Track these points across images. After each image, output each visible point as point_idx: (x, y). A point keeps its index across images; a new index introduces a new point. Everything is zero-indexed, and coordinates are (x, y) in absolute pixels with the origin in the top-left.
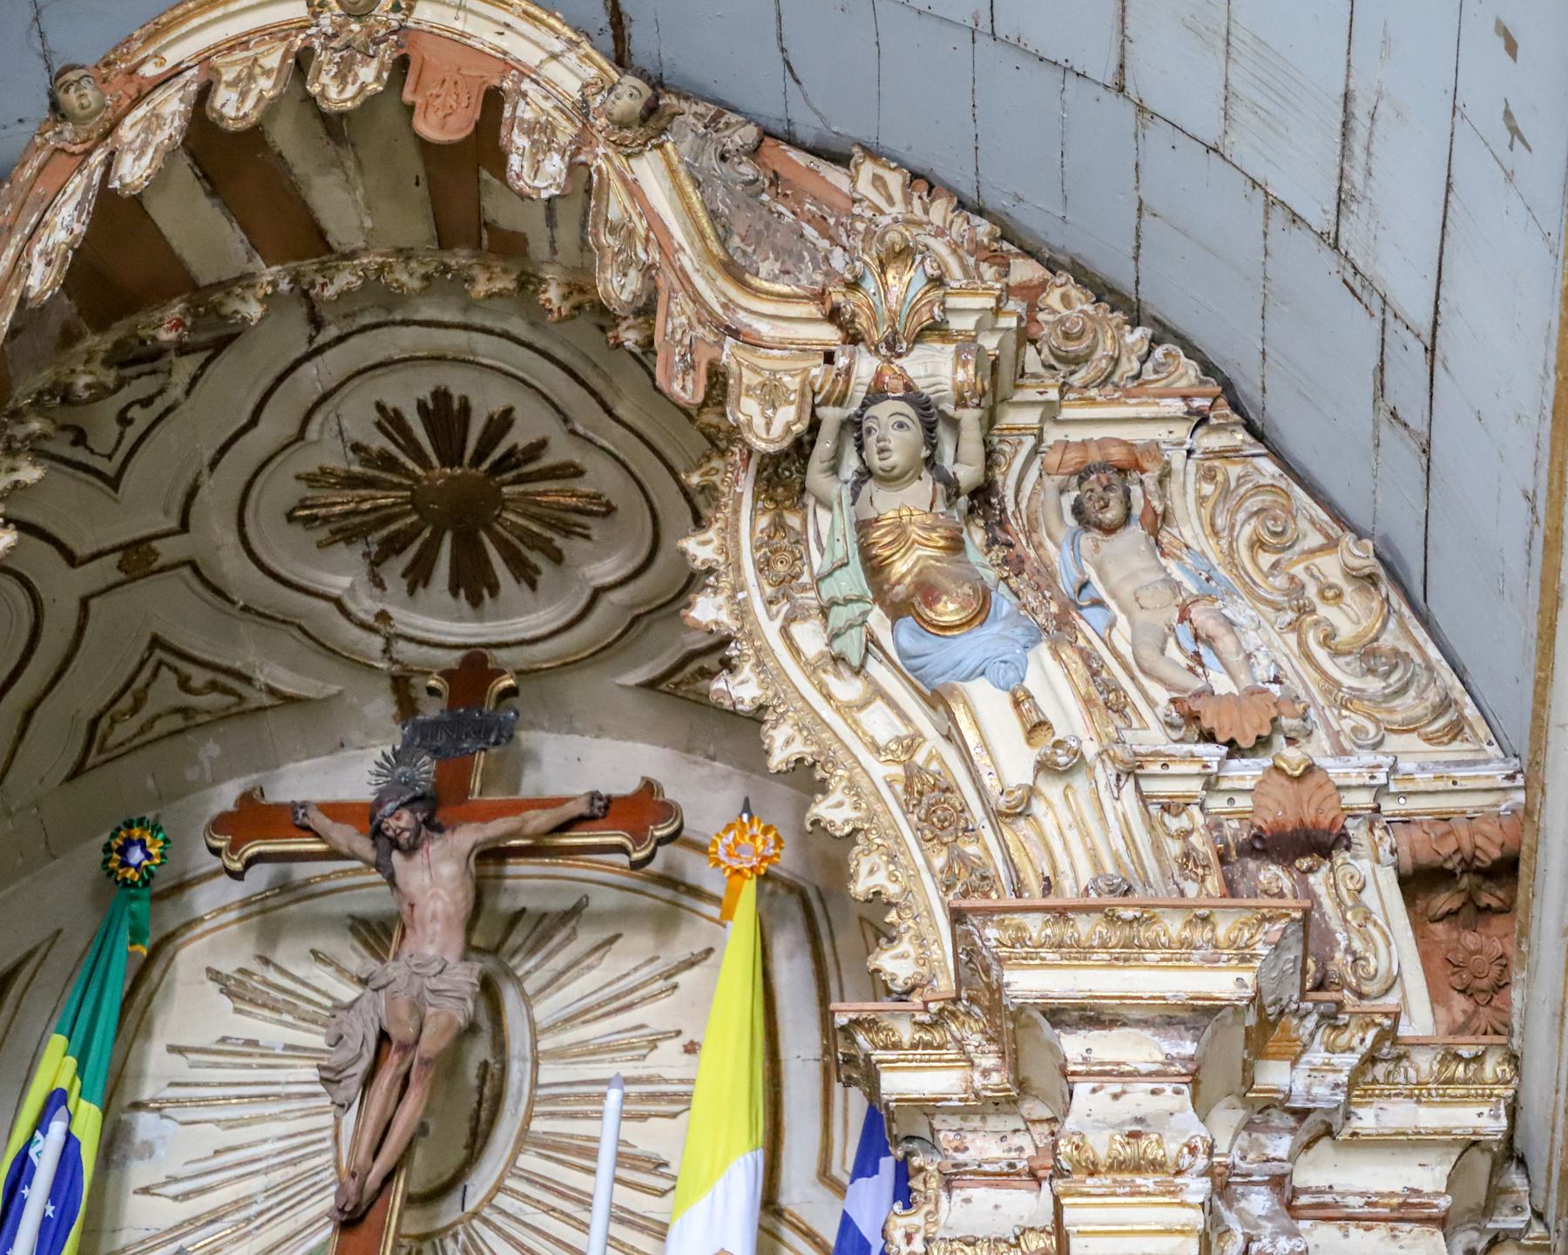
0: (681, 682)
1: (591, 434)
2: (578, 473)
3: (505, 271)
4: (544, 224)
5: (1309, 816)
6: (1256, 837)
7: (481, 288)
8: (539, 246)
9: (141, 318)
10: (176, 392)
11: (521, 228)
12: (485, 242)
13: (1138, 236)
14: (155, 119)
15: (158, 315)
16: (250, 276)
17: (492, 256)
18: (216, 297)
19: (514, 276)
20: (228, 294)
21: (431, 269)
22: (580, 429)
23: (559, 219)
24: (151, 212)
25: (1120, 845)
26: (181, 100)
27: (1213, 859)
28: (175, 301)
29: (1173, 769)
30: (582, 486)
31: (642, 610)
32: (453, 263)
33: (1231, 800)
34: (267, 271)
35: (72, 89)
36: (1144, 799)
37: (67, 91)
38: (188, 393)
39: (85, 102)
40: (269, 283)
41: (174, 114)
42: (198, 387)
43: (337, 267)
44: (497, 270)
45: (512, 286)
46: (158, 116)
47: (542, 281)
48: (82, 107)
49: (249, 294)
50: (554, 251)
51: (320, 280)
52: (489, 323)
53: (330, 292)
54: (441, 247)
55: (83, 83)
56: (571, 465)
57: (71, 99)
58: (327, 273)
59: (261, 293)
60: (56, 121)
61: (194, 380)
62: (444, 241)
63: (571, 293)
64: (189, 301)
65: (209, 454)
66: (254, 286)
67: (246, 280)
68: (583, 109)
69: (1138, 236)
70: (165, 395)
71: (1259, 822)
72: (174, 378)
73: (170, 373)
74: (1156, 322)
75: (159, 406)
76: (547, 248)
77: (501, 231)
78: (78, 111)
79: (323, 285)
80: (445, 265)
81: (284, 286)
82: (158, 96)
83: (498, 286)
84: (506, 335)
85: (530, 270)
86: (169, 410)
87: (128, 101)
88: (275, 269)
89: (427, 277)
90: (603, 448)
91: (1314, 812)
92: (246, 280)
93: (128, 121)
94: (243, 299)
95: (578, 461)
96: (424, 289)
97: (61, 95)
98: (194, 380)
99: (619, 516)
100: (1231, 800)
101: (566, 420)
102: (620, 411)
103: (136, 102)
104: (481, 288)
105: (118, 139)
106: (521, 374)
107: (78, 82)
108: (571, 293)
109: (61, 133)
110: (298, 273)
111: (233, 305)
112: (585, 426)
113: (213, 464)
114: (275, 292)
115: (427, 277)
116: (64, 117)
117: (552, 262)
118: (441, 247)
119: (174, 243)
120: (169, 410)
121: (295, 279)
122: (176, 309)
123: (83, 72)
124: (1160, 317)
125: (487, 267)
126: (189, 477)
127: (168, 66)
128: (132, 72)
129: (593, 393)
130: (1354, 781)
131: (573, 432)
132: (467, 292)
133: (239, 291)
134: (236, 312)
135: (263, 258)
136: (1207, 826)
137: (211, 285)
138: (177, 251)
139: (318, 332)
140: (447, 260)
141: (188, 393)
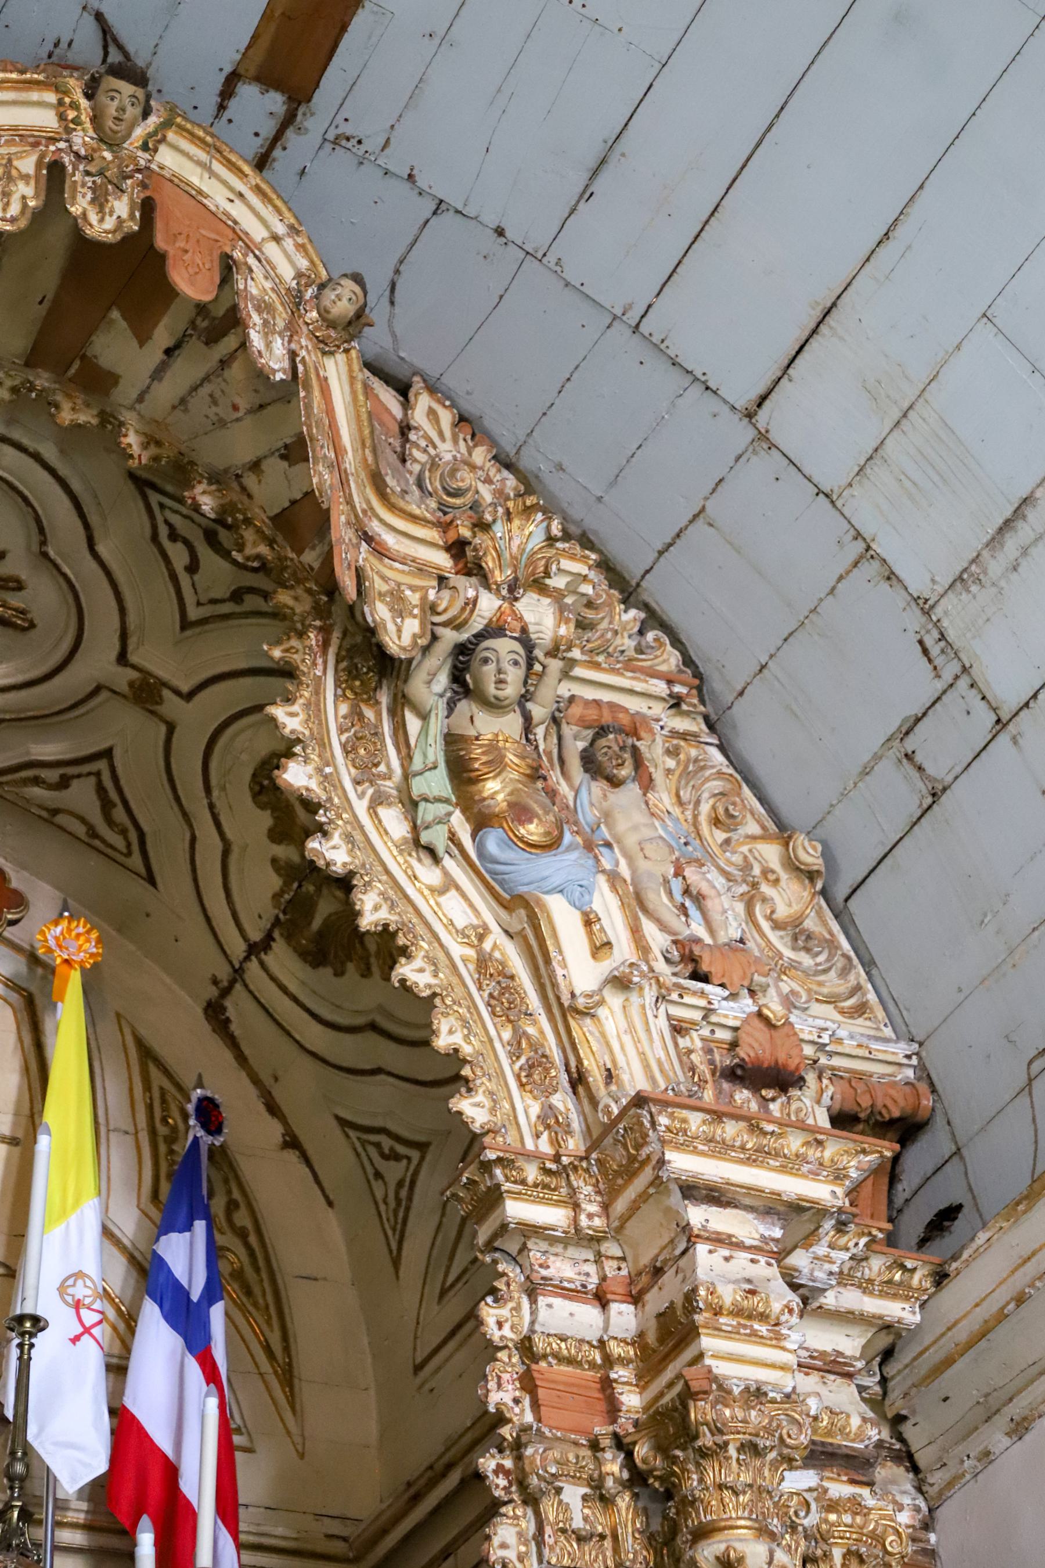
0: (7, 783)
1: (59, 561)
2: (19, 586)
3: (88, 405)
4: (149, 374)
5: (782, 1057)
6: (738, 1065)
7: (66, 416)
8: (125, 392)
11: (119, 371)
12: (72, 371)
13: (678, 536)
17: (72, 385)
19: (95, 412)
21: (17, 382)
22: (52, 553)
23: (169, 374)
25: (662, 1055)
27: (708, 1077)
29: (687, 999)
30: (15, 600)
31: (7, 717)
32: (37, 382)
33: (713, 1032)
36: (669, 1017)
44: (79, 401)
45: (95, 421)
47: (122, 424)
50: (141, 399)
52: (25, 441)
54: (27, 364)
56: (18, 581)
62: (32, 360)
63: (148, 443)
68: (296, 301)
69: (678, 536)
71: (742, 1055)
74: (646, 607)
76: (134, 395)
77: (97, 368)
80: (29, 382)
83: (82, 418)
84: (36, 457)
85: (108, 410)
89: (14, 390)
90: (64, 575)
91: (784, 1055)
95: (23, 577)
96: (11, 402)
99: (32, 634)
100: (713, 1032)
101: (44, 543)
102: (101, 549)
104: (66, 416)
106: (26, 493)
108: (148, 443)
112: (58, 553)
115: (14, 390)
117: (132, 408)
118: (27, 364)
124: (654, 605)
125: (69, 396)
129: (87, 526)
130: (807, 1037)
131: (45, 555)
132: (52, 416)
136: (703, 1049)
140: (31, 379)
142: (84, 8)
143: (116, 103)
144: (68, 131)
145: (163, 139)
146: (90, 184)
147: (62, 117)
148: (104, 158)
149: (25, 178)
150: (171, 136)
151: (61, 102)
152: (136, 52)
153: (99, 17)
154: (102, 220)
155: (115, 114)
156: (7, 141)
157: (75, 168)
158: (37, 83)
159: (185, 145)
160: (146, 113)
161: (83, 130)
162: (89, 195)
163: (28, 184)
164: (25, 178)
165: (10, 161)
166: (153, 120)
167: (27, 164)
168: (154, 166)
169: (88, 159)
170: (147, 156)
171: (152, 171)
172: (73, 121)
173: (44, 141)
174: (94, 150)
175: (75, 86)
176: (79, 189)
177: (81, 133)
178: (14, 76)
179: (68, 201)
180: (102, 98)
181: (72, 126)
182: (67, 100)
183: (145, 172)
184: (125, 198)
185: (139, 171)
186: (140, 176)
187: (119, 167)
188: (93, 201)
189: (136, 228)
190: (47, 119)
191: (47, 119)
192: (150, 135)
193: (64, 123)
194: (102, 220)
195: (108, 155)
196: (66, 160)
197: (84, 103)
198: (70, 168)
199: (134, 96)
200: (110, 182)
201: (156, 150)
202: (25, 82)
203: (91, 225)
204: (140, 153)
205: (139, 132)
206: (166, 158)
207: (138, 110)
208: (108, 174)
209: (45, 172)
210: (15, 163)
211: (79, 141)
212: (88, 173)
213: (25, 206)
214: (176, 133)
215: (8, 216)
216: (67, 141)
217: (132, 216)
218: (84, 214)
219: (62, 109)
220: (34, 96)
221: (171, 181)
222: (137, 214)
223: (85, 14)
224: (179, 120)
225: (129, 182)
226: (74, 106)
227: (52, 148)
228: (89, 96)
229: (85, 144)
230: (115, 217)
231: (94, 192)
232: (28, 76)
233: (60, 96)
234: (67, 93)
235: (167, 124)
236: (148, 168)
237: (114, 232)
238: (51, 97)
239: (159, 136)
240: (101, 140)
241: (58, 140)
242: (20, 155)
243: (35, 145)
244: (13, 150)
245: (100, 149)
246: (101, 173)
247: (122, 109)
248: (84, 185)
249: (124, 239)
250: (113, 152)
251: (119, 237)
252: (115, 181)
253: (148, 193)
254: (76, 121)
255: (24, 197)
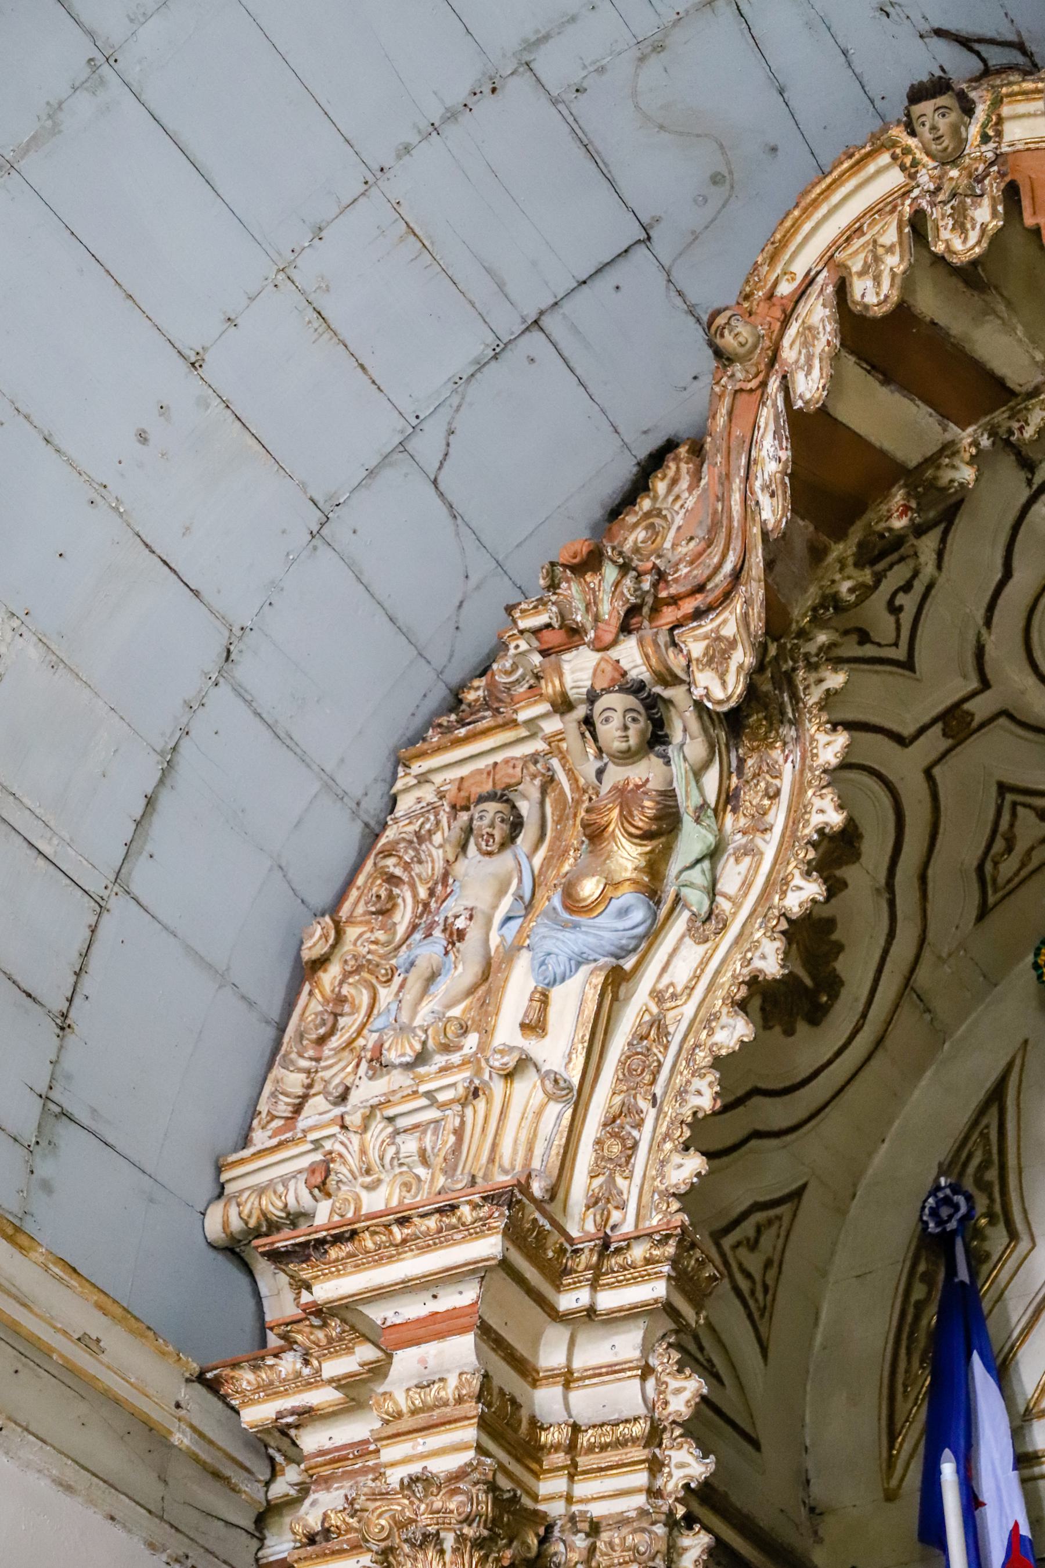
9: (870, 516)
10: (929, 569)
14: (809, 332)
15: (884, 508)
16: (952, 443)
18: (929, 473)
20: (938, 467)
24: (840, 418)
26: (824, 306)
28: (894, 490)
34: (964, 434)
35: (726, 332)
37: (722, 336)
38: (939, 567)
39: (741, 339)
40: (970, 445)
41: (822, 320)
42: (946, 558)
43: (1026, 409)
46: (810, 328)
48: (742, 345)
49: (957, 462)
51: (1016, 425)
53: (1029, 432)
55: (733, 322)
57: (728, 341)
58: (1019, 416)
59: (967, 457)
60: (725, 366)
61: (940, 555)
64: (906, 486)
65: (980, 615)
66: (958, 452)
67: (949, 449)
70: (921, 576)
72: (922, 559)
73: (916, 554)
75: (919, 587)
78: (741, 351)
79: (1021, 429)
81: (985, 442)
82: (802, 309)
86: (930, 587)
87: (779, 324)
88: (970, 430)
92: (949, 449)
93: (786, 342)
94: (954, 467)
97: (718, 341)
98: (940, 555)
103: (785, 323)
105: (785, 363)
107: (728, 323)
109: (733, 376)
110: (993, 427)
111: (946, 476)
113: (988, 622)
114: (979, 451)
116: (731, 361)
119: (873, 439)
120: (930, 587)
121: (993, 433)
122: (898, 497)
123: (728, 313)
126: (971, 637)
127: (799, 278)
128: (770, 296)
133: (947, 460)
134: (952, 481)
135: (956, 424)
137: (920, 465)
138: (878, 444)
139: (1033, 473)
141: (939, 567)
142: (921, 36)
143: (928, 125)
144: (912, 176)
145: (1000, 121)
146: (949, 211)
147: (903, 168)
148: (952, 179)
149: (890, 250)
150: (1006, 110)
151: (894, 157)
152: (999, 33)
153: (939, 33)
154: (965, 241)
155: (931, 136)
156: (870, 224)
157: (933, 204)
158: (869, 155)
159: (1022, 108)
160: (968, 109)
161: (924, 166)
162: (951, 222)
163: (893, 253)
164: (890, 250)
165: (875, 242)
166: (981, 111)
167: (890, 236)
168: (1005, 149)
169: (939, 189)
170: (992, 145)
171: (1007, 154)
172: (912, 166)
173: (899, 201)
174: (940, 178)
175: (898, 133)
176: (941, 223)
177: (924, 171)
178: (846, 165)
179: (931, 244)
180: (919, 129)
181: (913, 170)
182: (898, 151)
183: (1000, 160)
184: (986, 201)
185: (992, 164)
186: (995, 168)
187: (970, 176)
188: (953, 229)
189: (1001, 223)
190: (895, 178)
191: (895, 178)
192: (984, 126)
193: (907, 172)
194: (965, 241)
195: (954, 173)
196: (924, 204)
197: (912, 142)
198: (929, 210)
199: (938, 108)
200: (966, 196)
201: (999, 134)
202: (858, 163)
203: (955, 253)
204: (984, 148)
205: (974, 131)
206: (1016, 133)
207: (953, 117)
208: (960, 191)
209: (907, 230)
210: (882, 240)
211: (926, 178)
212: (944, 203)
213: (894, 275)
214: (1010, 103)
215: (882, 297)
216: (918, 186)
217: (994, 214)
218: (948, 247)
219: (899, 162)
220: (871, 168)
221: (1028, 149)
222: (1000, 208)
223: (927, 40)
224: (1004, 90)
225: (986, 182)
226: (907, 151)
227: (908, 202)
228: (913, 133)
229: (931, 177)
230: (978, 227)
231: (953, 218)
232: (857, 156)
233: (891, 151)
234: (894, 144)
235: (997, 102)
236: (1002, 154)
237: (979, 242)
238: (885, 158)
239: (994, 118)
240: (943, 164)
241: (910, 191)
242: (883, 231)
243: (892, 212)
244: (877, 228)
245: (946, 173)
246: (954, 195)
247: (934, 128)
248: (943, 217)
249: (990, 244)
250: (957, 166)
251: (985, 244)
252: (969, 192)
253: (1008, 179)
254: (915, 163)
255: (891, 269)
